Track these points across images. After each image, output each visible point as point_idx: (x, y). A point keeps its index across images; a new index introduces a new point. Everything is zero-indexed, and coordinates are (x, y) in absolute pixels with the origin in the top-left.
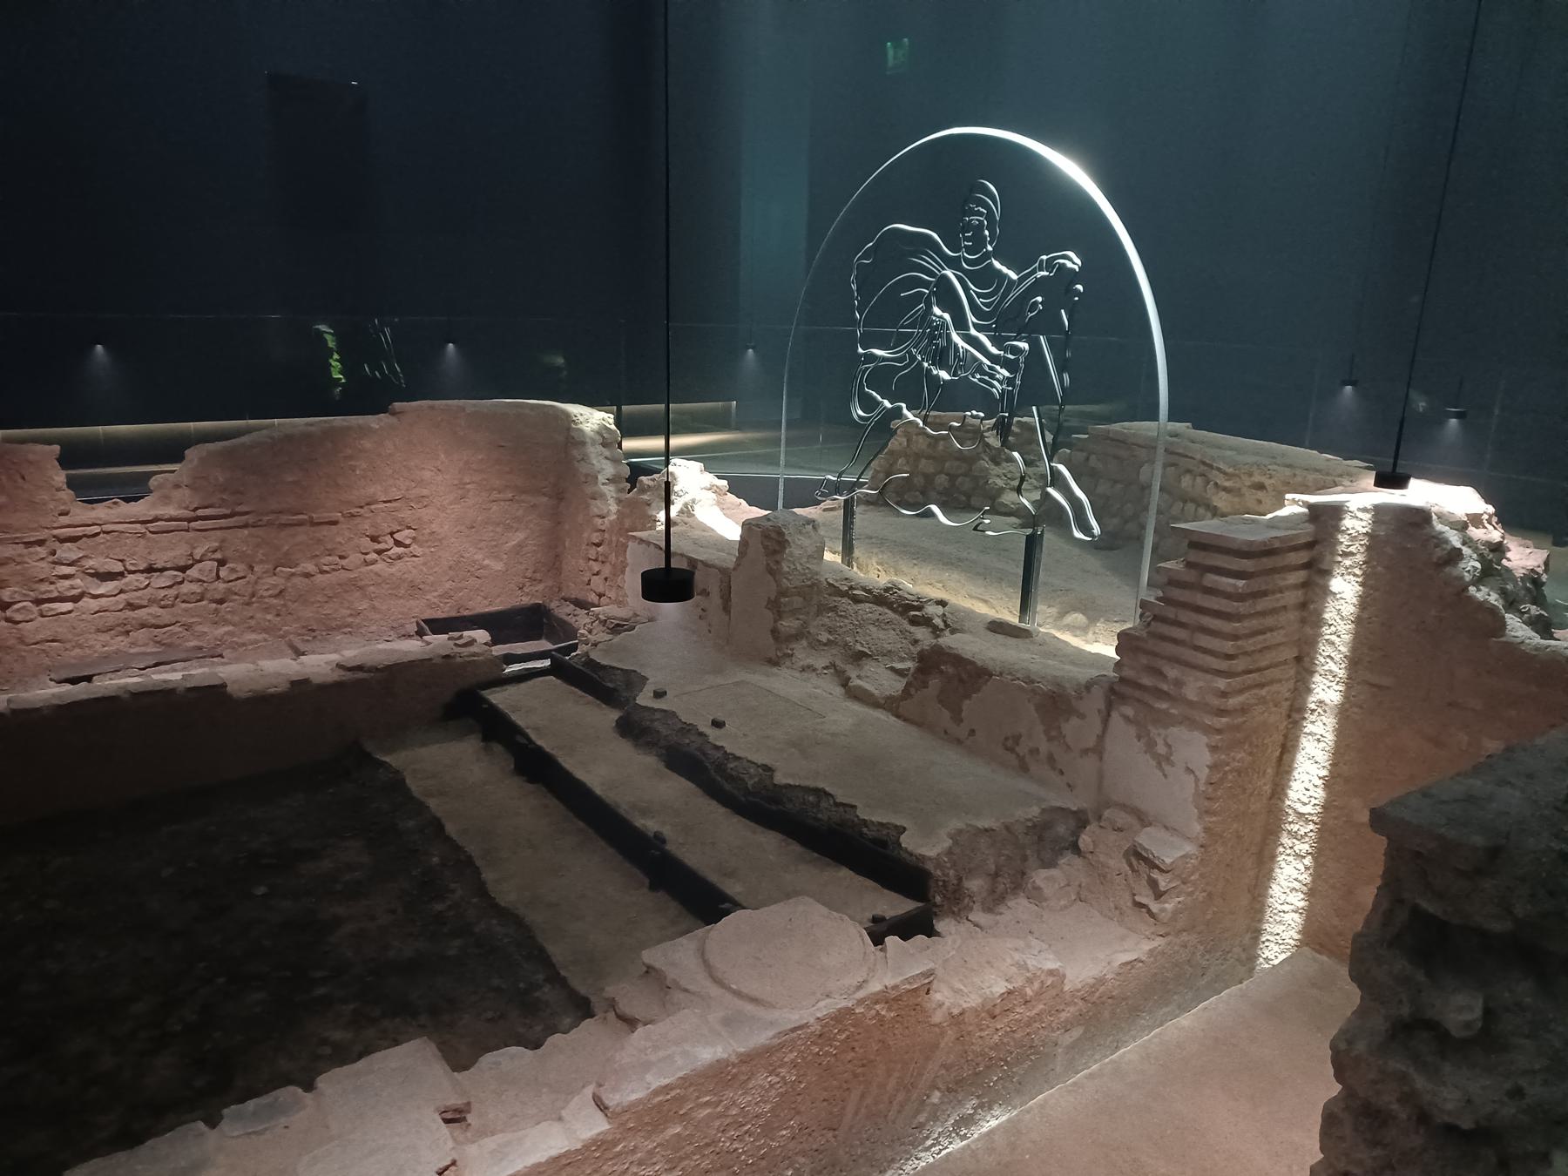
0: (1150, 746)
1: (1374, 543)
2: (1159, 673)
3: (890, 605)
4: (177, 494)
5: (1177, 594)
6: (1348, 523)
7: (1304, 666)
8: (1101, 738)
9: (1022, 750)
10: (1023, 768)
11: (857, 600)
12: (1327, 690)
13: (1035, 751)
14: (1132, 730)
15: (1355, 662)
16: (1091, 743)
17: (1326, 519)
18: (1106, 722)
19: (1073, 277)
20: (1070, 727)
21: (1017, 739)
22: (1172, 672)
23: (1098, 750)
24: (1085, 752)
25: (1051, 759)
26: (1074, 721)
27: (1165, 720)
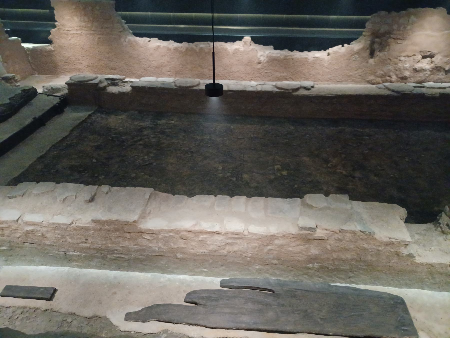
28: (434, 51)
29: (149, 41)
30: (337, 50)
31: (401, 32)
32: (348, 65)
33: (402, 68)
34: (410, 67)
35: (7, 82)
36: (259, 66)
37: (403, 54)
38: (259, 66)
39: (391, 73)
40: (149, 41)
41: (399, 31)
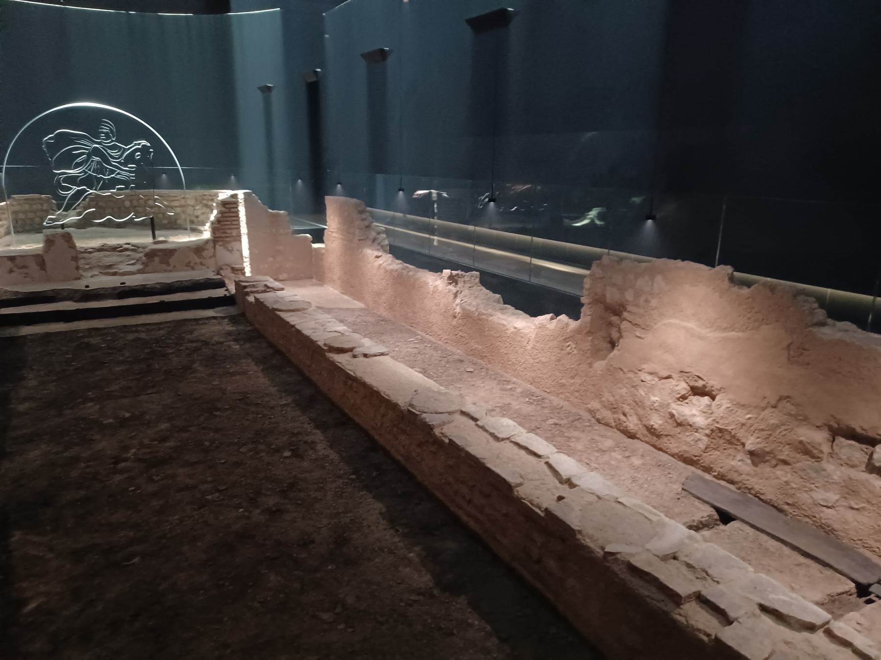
0: (228, 249)
1: (245, 200)
7: (238, 228)
10: (193, 269)
11: (90, 253)
12: (244, 229)
13: (196, 263)
15: (248, 223)
18: (215, 248)
20: (205, 254)
21: (190, 263)
22: (229, 231)
23: (214, 255)
24: (211, 257)
25: (201, 264)
27: (229, 242)
28: (714, 382)
29: (378, 257)
30: (545, 322)
31: (642, 311)
32: (559, 361)
33: (648, 403)
34: (661, 405)
36: (454, 322)
37: (646, 367)
38: (454, 322)
39: (627, 409)
40: (378, 257)
41: (637, 306)
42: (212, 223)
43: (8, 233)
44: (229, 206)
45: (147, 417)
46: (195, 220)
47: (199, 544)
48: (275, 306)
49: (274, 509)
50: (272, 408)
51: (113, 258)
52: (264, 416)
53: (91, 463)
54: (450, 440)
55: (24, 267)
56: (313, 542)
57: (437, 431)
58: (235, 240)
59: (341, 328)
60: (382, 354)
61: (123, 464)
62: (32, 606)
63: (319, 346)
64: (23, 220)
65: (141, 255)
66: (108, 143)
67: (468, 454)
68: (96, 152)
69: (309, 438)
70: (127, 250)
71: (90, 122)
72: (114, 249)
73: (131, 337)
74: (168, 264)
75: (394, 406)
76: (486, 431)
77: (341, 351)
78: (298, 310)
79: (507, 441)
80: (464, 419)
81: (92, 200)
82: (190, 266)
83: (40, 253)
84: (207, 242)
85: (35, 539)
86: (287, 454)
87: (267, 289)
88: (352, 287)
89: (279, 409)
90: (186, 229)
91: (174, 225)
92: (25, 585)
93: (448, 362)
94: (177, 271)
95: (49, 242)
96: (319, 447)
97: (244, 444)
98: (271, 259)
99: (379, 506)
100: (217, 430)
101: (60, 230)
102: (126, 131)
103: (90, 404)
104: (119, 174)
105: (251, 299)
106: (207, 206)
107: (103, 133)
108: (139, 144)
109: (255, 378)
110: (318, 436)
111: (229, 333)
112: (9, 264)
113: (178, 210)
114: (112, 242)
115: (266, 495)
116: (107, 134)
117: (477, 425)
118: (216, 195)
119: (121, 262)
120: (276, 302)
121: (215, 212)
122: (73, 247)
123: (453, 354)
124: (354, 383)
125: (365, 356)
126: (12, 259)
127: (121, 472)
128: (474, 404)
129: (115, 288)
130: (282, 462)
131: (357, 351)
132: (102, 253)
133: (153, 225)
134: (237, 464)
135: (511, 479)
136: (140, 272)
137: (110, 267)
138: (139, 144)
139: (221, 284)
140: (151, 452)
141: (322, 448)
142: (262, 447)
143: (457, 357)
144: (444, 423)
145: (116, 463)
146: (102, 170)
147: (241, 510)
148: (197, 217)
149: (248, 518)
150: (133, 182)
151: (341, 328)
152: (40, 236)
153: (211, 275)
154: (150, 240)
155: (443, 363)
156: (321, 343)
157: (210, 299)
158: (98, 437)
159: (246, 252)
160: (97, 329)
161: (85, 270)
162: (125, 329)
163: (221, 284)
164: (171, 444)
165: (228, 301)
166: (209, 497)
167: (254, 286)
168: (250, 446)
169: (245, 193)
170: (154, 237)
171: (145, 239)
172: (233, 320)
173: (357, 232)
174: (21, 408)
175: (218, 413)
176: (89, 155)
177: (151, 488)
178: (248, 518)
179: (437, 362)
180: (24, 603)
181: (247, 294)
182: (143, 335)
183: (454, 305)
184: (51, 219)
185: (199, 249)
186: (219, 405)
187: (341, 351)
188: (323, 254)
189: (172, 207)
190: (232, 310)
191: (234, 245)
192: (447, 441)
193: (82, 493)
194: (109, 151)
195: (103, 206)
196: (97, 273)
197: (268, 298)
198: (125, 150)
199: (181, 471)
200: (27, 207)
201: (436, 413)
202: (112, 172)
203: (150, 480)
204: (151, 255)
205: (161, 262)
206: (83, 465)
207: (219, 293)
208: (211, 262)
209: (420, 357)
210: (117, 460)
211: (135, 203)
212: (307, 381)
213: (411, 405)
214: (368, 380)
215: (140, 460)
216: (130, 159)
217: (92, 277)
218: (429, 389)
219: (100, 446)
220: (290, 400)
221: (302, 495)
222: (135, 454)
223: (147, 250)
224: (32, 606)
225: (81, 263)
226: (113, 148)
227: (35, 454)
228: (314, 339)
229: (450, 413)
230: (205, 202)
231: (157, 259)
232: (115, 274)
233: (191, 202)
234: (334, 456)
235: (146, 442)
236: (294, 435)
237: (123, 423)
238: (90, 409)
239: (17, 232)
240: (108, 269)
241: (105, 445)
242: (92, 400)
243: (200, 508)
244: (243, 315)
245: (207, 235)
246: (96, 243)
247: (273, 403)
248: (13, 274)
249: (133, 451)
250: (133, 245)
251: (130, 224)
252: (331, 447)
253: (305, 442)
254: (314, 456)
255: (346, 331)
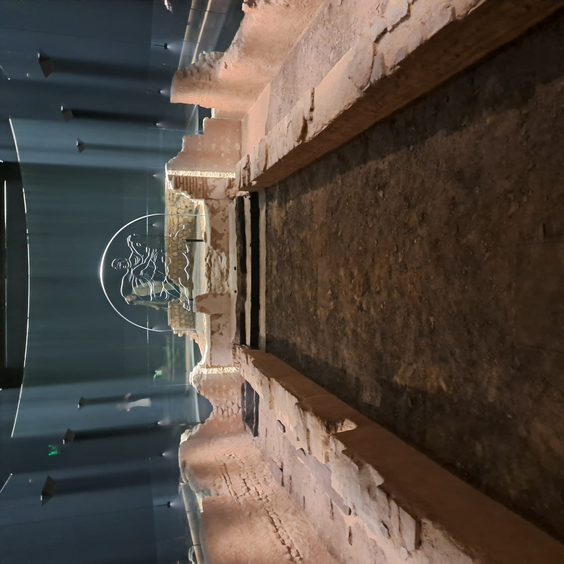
0: (213, 189)
1: (173, 169)
2: (200, 188)
3: (210, 274)
4: (217, 484)
5: (185, 187)
6: (171, 174)
8: (215, 200)
9: (224, 218)
10: (227, 217)
11: (211, 285)
12: (198, 174)
14: (211, 193)
16: (216, 202)
17: (170, 177)
18: (211, 199)
19: (132, 236)
20: (216, 207)
21: (222, 219)
22: (199, 187)
23: (218, 200)
24: (219, 203)
25: (224, 210)
26: (214, 206)
27: (207, 187)
35: (232, 188)
42: (192, 198)
43: (195, 331)
44: (179, 183)
45: (334, 280)
46: (189, 209)
47: (432, 277)
48: (262, 169)
49: (421, 218)
50: (343, 192)
51: (216, 272)
52: (347, 201)
53: (359, 324)
54: (398, 64)
55: (219, 326)
56: (453, 198)
57: (389, 73)
58: (206, 182)
59: (285, 121)
60: (313, 94)
61: (364, 306)
62: (444, 386)
63: (298, 146)
64: (186, 321)
65: (215, 252)
66: (129, 264)
67: (414, 52)
68: (136, 273)
69: (372, 173)
70: (210, 261)
71: (113, 277)
72: (209, 269)
73: (274, 272)
74: (223, 234)
75: (359, 102)
76: (398, 24)
77: (305, 130)
78: (267, 151)
79: (412, 7)
80: (383, 41)
81: (172, 277)
82: (225, 219)
83: (209, 315)
84: (207, 204)
85: (402, 369)
86: (381, 194)
87: (247, 168)
88: (251, 91)
89: (344, 187)
90: (196, 217)
91: (193, 225)
92: (429, 385)
93: (329, 21)
94: (228, 228)
95: (202, 310)
96: (381, 167)
97: (367, 223)
98: (223, 155)
99: (440, 134)
100: (352, 238)
101: (194, 302)
102: (120, 250)
103: (318, 312)
104: (153, 259)
105: (254, 183)
106: (178, 198)
107: (122, 267)
108: (130, 243)
109: (317, 197)
110: (371, 164)
111: (280, 205)
112: (216, 334)
113: (181, 220)
114: (204, 269)
115: (408, 220)
116: (123, 264)
117: (391, 31)
118: (169, 191)
119: (219, 266)
120: (258, 166)
121: (183, 194)
122: (206, 296)
123: (322, 12)
124: (334, 126)
125: (312, 110)
126: (212, 333)
127: (369, 309)
128: (371, 25)
129: (238, 275)
130: (387, 200)
131: (307, 116)
132: (212, 277)
133: (192, 240)
134: (381, 232)
135: (446, 20)
136: (227, 254)
137: (222, 273)
138: (130, 243)
139: (241, 200)
140: (359, 286)
141: (383, 165)
142: (371, 211)
143: (326, 10)
144: (383, 64)
145: (362, 310)
146: (150, 270)
147: (415, 241)
148: (187, 207)
149: (422, 238)
150: (159, 251)
151: (285, 121)
152: (198, 314)
153: (233, 205)
154: (203, 243)
155: (329, 27)
156: (296, 144)
157: (252, 211)
158: (342, 314)
159: (216, 175)
160: (267, 292)
161: (223, 290)
162: (268, 274)
163: (241, 200)
164: (356, 273)
165: (254, 197)
166: (400, 259)
167: (244, 178)
168: (369, 219)
169: (168, 169)
170: (201, 241)
171: (203, 249)
172: (269, 198)
173: (202, 81)
174: (314, 351)
175: (339, 233)
176: (139, 277)
177: (384, 294)
178: (422, 238)
179: (328, 32)
180: (440, 389)
181: (250, 184)
182: (275, 263)
183: (277, 5)
184: (186, 307)
185: (212, 211)
186: (334, 230)
187: (305, 130)
188: (221, 111)
189: (179, 224)
190: (262, 197)
191: (210, 183)
192: (398, 67)
193: (378, 336)
194: (136, 264)
195: (178, 272)
196: (226, 283)
197: (255, 172)
198: (135, 253)
199: (377, 272)
200: (176, 318)
201: (372, 68)
202: (151, 263)
203: (378, 293)
204: (215, 245)
205: (221, 239)
206: (359, 329)
207: (247, 202)
208: (223, 203)
209: (320, 48)
210: (360, 308)
211: (175, 249)
212: (326, 157)
213: (361, 88)
214: (333, 115)
215: (363, 295)
216: (141, 250)
217: (229, 286)
218: (350, 65)
219: (348, 316)
220: (338, 176)
221: (415, 193)
222: (358, 297)
223: (211, 248)
224: (444, 386)
225: (219, 292)
226: (133, 260)
227: (346, 352)
228: (292, 148)
229: (375, 55)
230: (175, 199)
231: (218, 242)
232: (228, 271)
233: (175, 210)
234: (390, 157)
235: (351, 286)
236: (367, 183)
237: (334, 297)
238: (322, 313)
239: (194, 326)
240: (224, 275)
241: (347, 313)
242: (316, 310)
243: (406, 268)
244: (266, 189)
245: (201, 203)
246: (204, 280)
247: (339, 190)
248: (223, 333)
249: (356, 297)
250: (207, 256)
251: (191, 257)
252: (383, 157)
253: (375, 176)
254: (388, 174)
255: (289, 117)
